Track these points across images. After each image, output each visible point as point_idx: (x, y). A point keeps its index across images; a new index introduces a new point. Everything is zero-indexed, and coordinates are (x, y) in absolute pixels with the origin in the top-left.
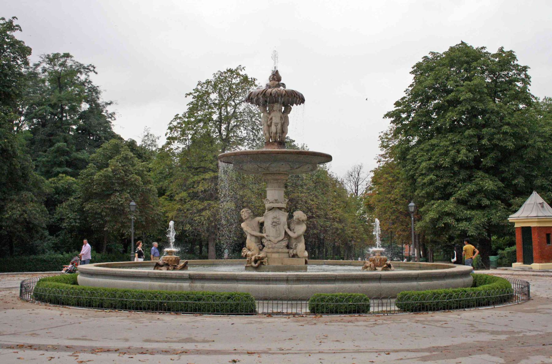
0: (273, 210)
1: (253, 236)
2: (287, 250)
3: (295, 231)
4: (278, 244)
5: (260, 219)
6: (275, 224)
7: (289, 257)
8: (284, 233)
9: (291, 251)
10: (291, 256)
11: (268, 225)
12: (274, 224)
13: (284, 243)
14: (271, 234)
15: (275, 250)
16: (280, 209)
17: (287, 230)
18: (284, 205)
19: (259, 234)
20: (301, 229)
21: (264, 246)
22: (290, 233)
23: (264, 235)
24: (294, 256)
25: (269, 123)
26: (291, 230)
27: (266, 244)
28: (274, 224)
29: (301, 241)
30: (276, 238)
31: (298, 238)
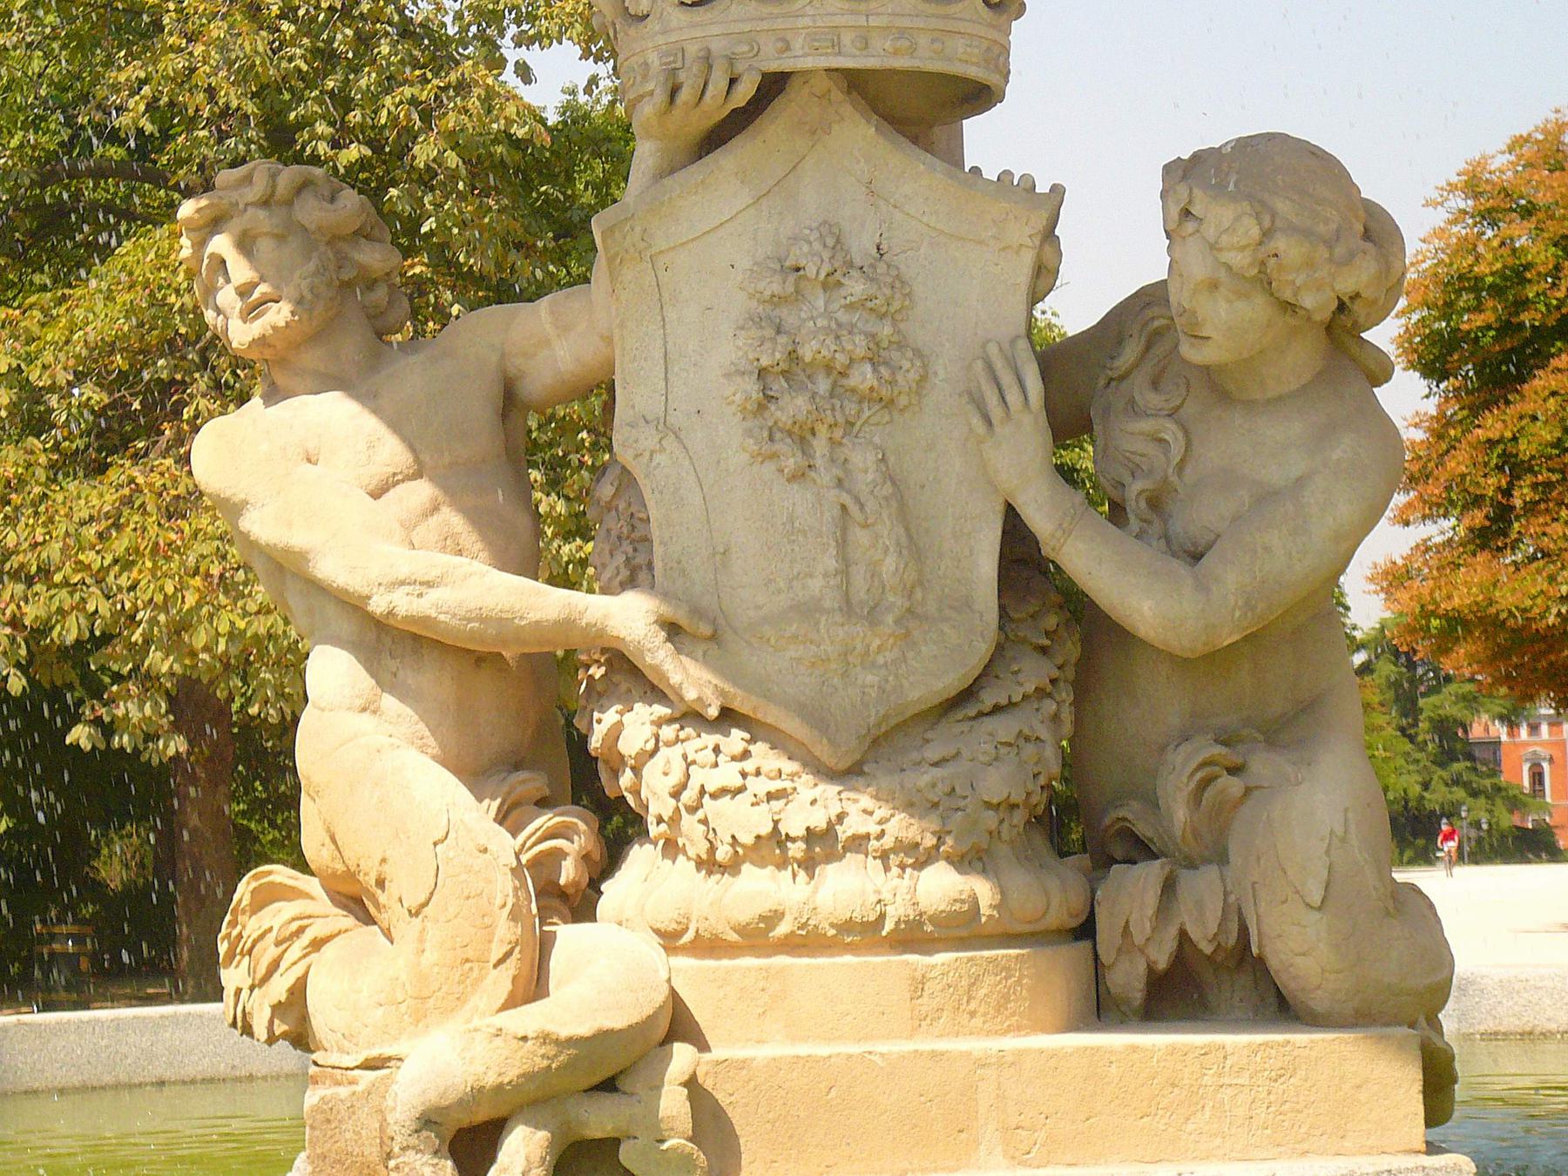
0: (775, 127)
3: (1199, 515)
5: (548, 338)
7: (1101, 1008)
8: (986, 565)
9: (1132, 894)
10: (1128, 978)
12: (793, 407)
15: (846, 887)
21: (619, 828)
27: (654, 790)
28: (793, 407)
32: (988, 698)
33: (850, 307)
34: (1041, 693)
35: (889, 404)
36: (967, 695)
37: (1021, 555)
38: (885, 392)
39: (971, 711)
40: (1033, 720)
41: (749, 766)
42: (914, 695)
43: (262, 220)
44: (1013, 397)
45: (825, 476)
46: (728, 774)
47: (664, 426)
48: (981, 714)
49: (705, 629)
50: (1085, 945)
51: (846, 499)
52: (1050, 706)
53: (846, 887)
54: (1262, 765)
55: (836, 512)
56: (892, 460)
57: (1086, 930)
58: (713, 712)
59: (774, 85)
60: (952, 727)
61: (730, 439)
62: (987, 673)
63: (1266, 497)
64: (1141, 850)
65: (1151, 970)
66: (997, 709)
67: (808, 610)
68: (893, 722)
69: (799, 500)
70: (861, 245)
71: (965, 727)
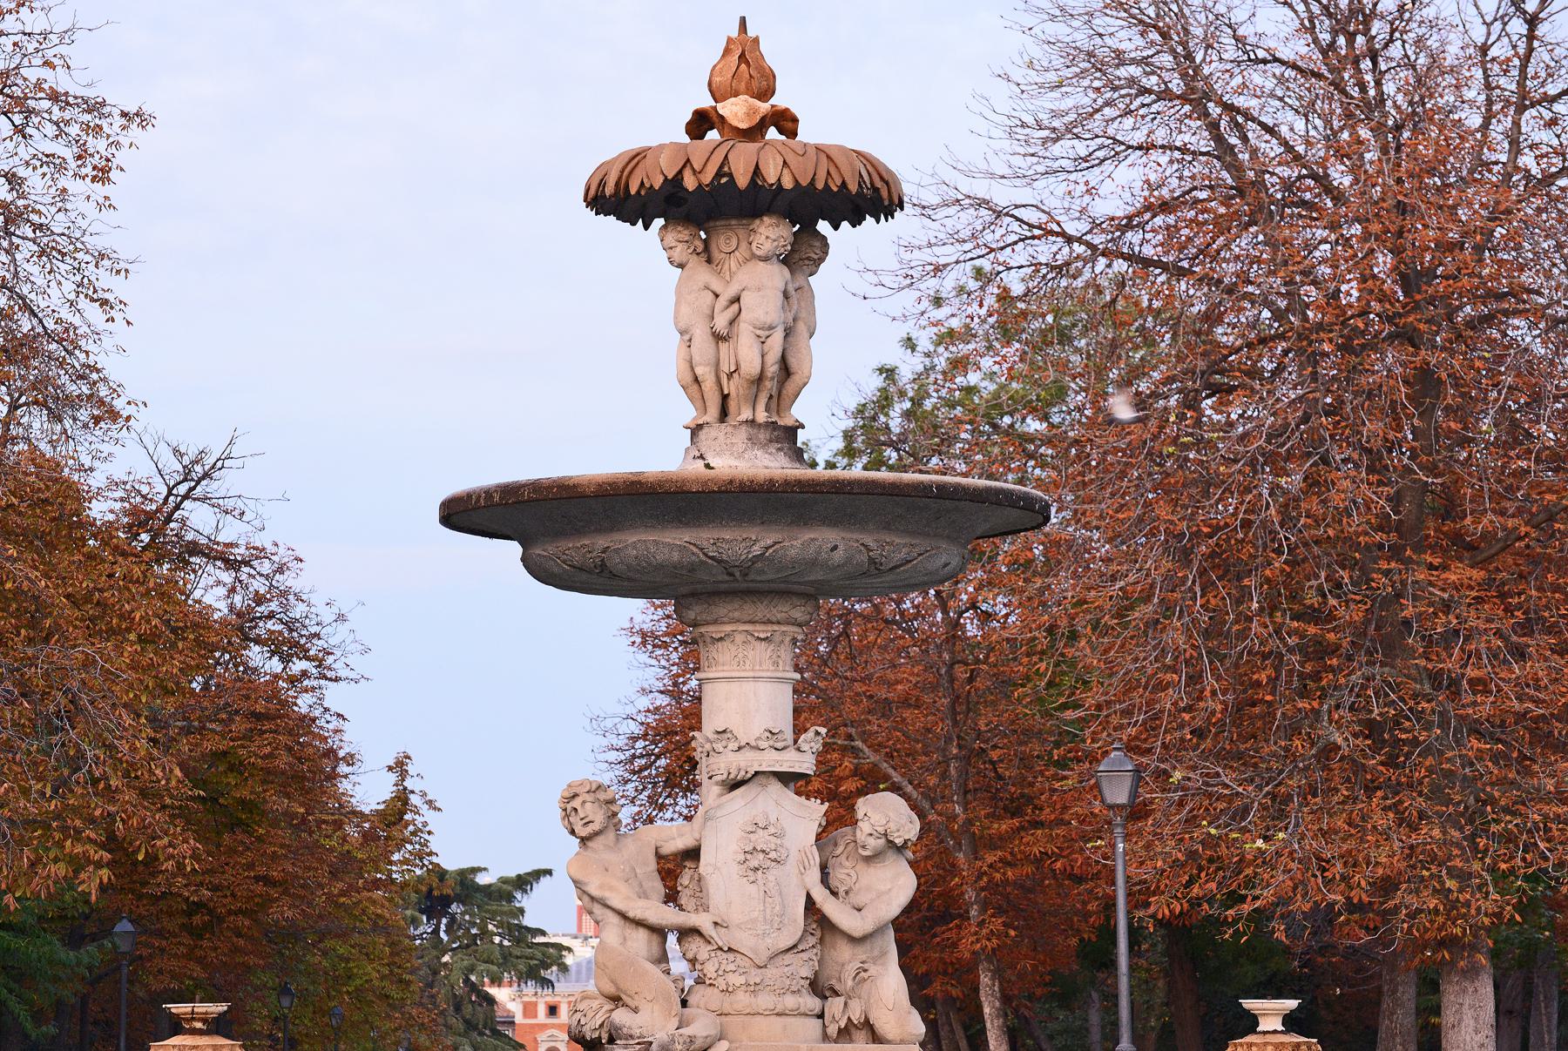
1: (639, 923)
2: (813, 1003)
4: (771, 972)
6: (759, 860)
7: (825, 1037)
9: (835, 1006)
10: (832, 1030)
11: (720, 867)
13: (802, 967)
14: (735, 916)
15: (765, 1001)
16: (785, 778)
17: (820, 894)
18: (804, 763)
19: (667, 915)
20: (896, 886)
22: (833, 909)
23: (702, 921)
24: (845, 1034)
25: (721, 323)
26: (834, 894)
29: (884, 954)
32: (801, 947)
36: (795, 946)
37: (810, 905)
43: (589, 797)
45: (760, 882)
46: (732, 967)
47: (716, 868)
53: (765, 1001)
54: (873, 970)
57: (821, 1016)
59: (757, 773)
60: (788, 958)
61: (735, 869)
62: (800, 940)
63: (880, 895)
64: (836, 994)
67: (754, 921)
69: (753, 887)
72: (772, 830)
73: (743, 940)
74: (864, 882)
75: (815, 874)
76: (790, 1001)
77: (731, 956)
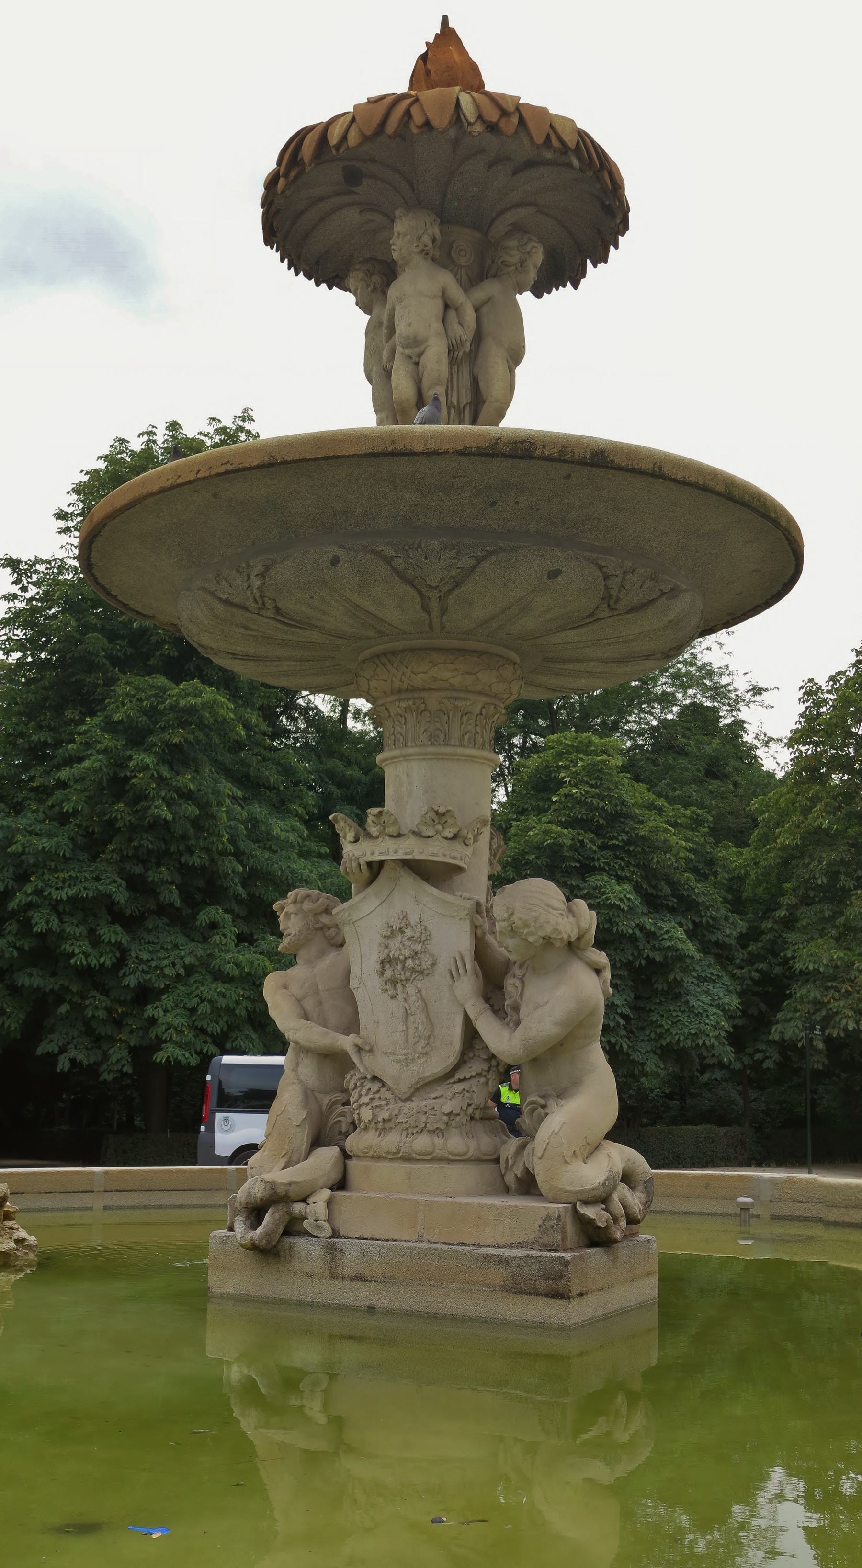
2: (483, 1141)
4: (418, 1103)
10: (510, 1179)
30: (407, 1062)
31: (550, 1061)
32: (459, 1075)
33: (409, 939)
34: (479, 1075)
35: (421, 972)
38: (418, 968)
39: (451, 1081)
40: (474, 1085)
41: (377, 1096)
42: (427, 1074)
44: (461, 970)
45: (401, 997)
48: (454, 1083)
49: (367, 1048)
50: (494, 1166)
51: (406, 1005)
52: (483, 1080)
53: (392, 1140)
54: (551, 1103)
55: (403, 1010)
56: (424, 992)
57: (497, 1161)
58: (369, 1077)
61: (376, 982)
65: (516, 1175)
66: (460, 1081)
68: (422, 1083)
69: (393, 1004)
70: (413, 919)
71: (449, 1086)
72: (408, 933)
73: (386, 1067)
74: (527, 993)
75: (467, 988)
76: (422, 1142)
77: (375, 1086)
